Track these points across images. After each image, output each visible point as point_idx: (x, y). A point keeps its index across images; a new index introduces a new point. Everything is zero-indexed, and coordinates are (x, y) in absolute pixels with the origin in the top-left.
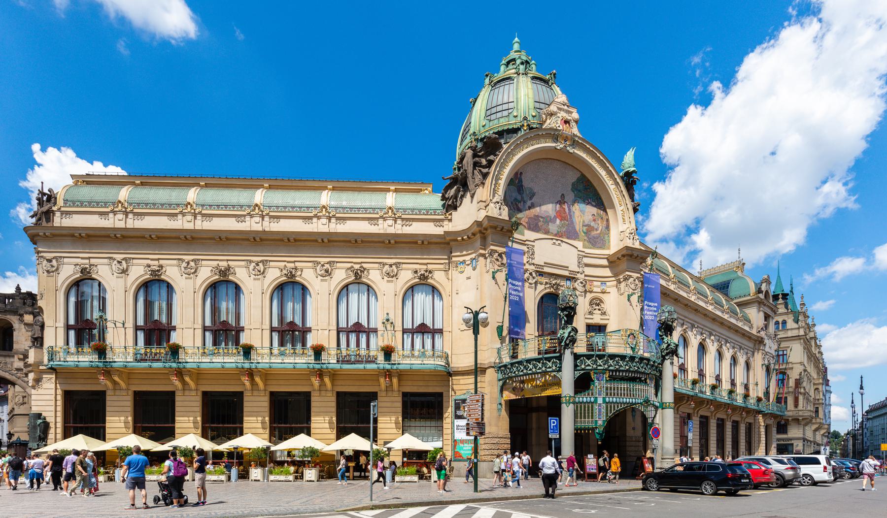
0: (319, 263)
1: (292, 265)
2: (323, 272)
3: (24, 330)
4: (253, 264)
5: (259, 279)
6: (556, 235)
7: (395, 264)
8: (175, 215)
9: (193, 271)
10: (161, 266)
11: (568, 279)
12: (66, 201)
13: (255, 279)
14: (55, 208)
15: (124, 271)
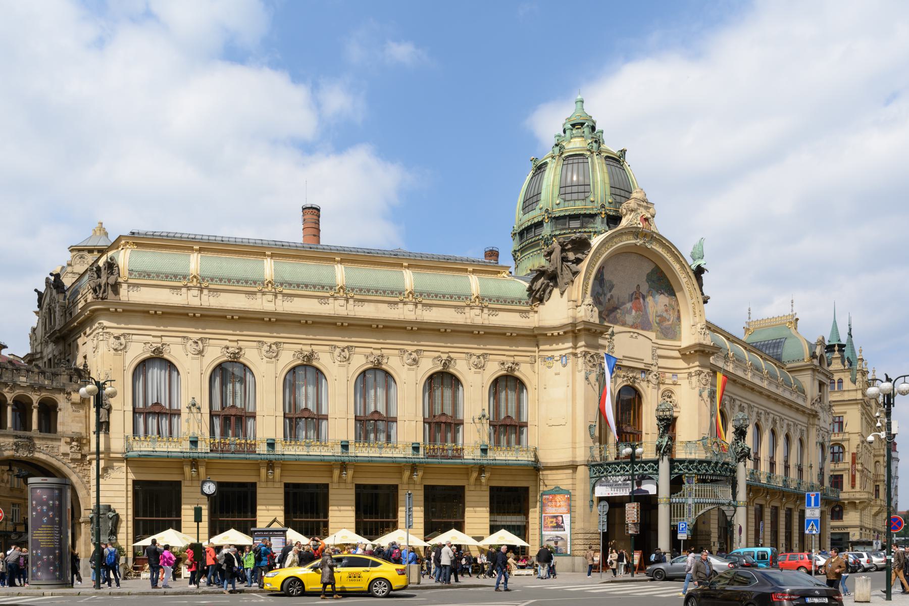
0: (405, 351)
1: (378, 352)
2: (410, 361)
3: (70, 410)
4: (338, 350)
5: (343, 366)
6: (631, 327)
7: (483, 355)
8: (254, 293)
9: (274, 354)
10: (240, 349)
11: (643, 371)
12: (131, 272)
13: (340, 366)
14: (120, 280)
15: (201, 353)
